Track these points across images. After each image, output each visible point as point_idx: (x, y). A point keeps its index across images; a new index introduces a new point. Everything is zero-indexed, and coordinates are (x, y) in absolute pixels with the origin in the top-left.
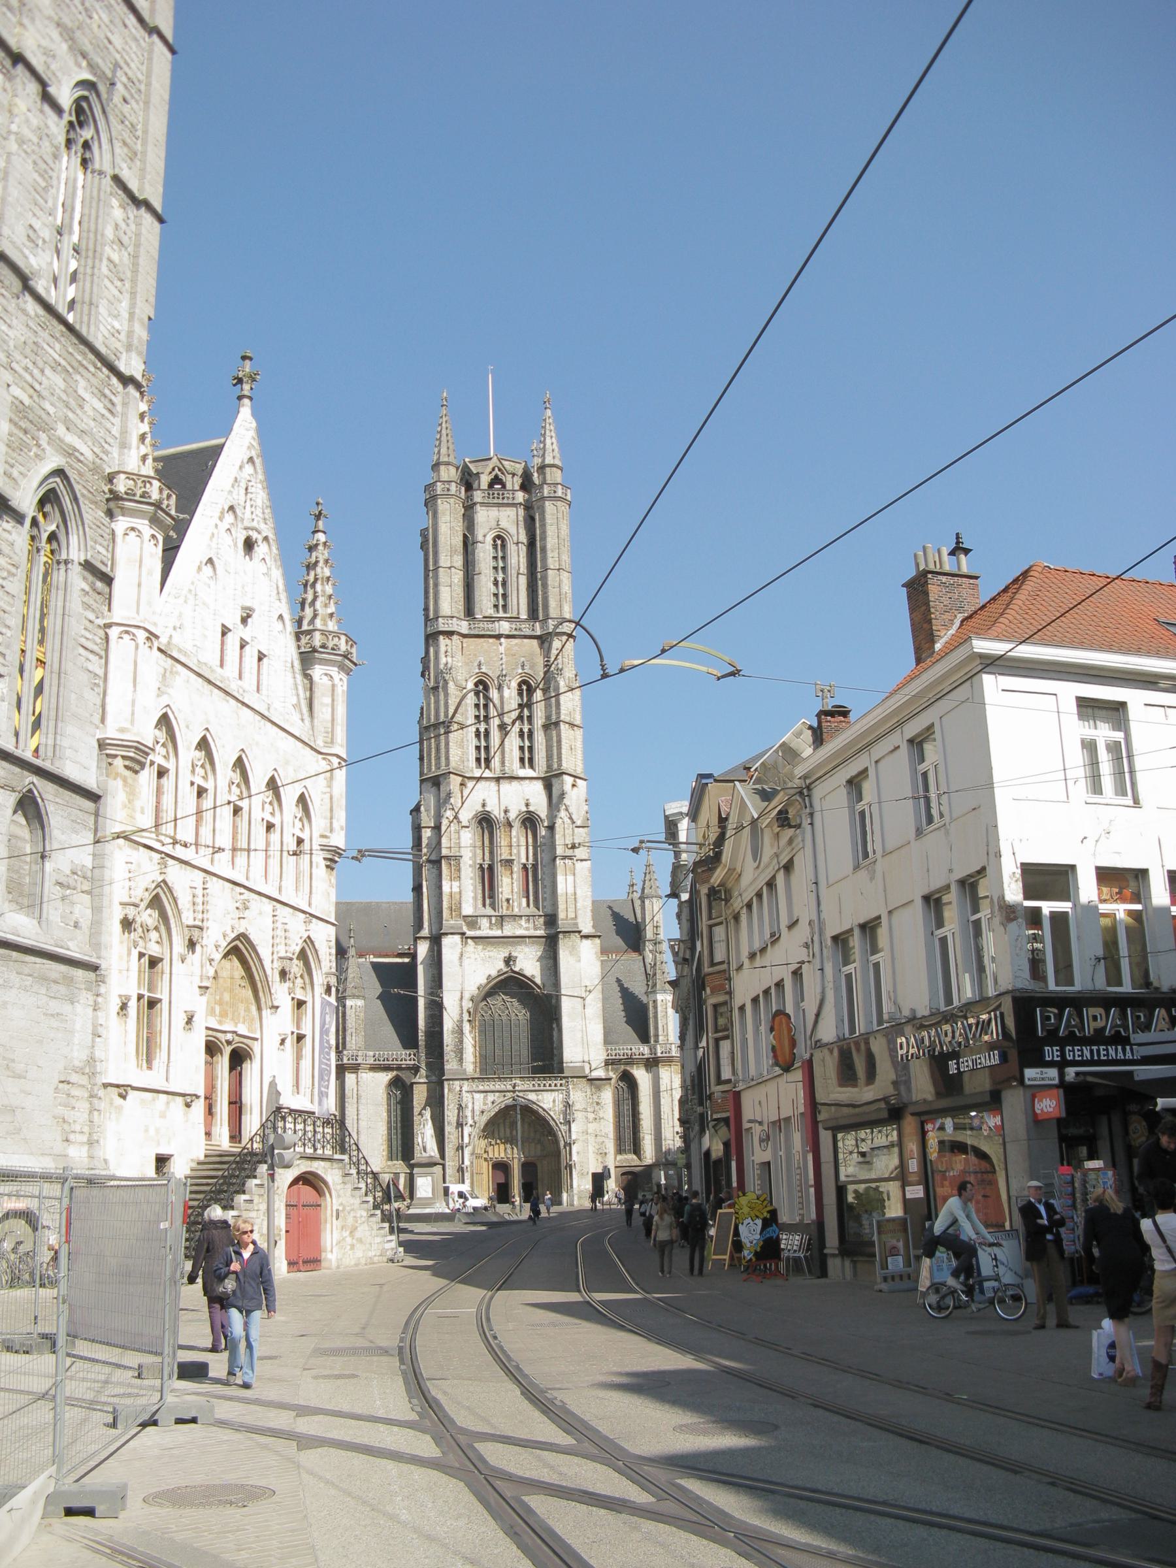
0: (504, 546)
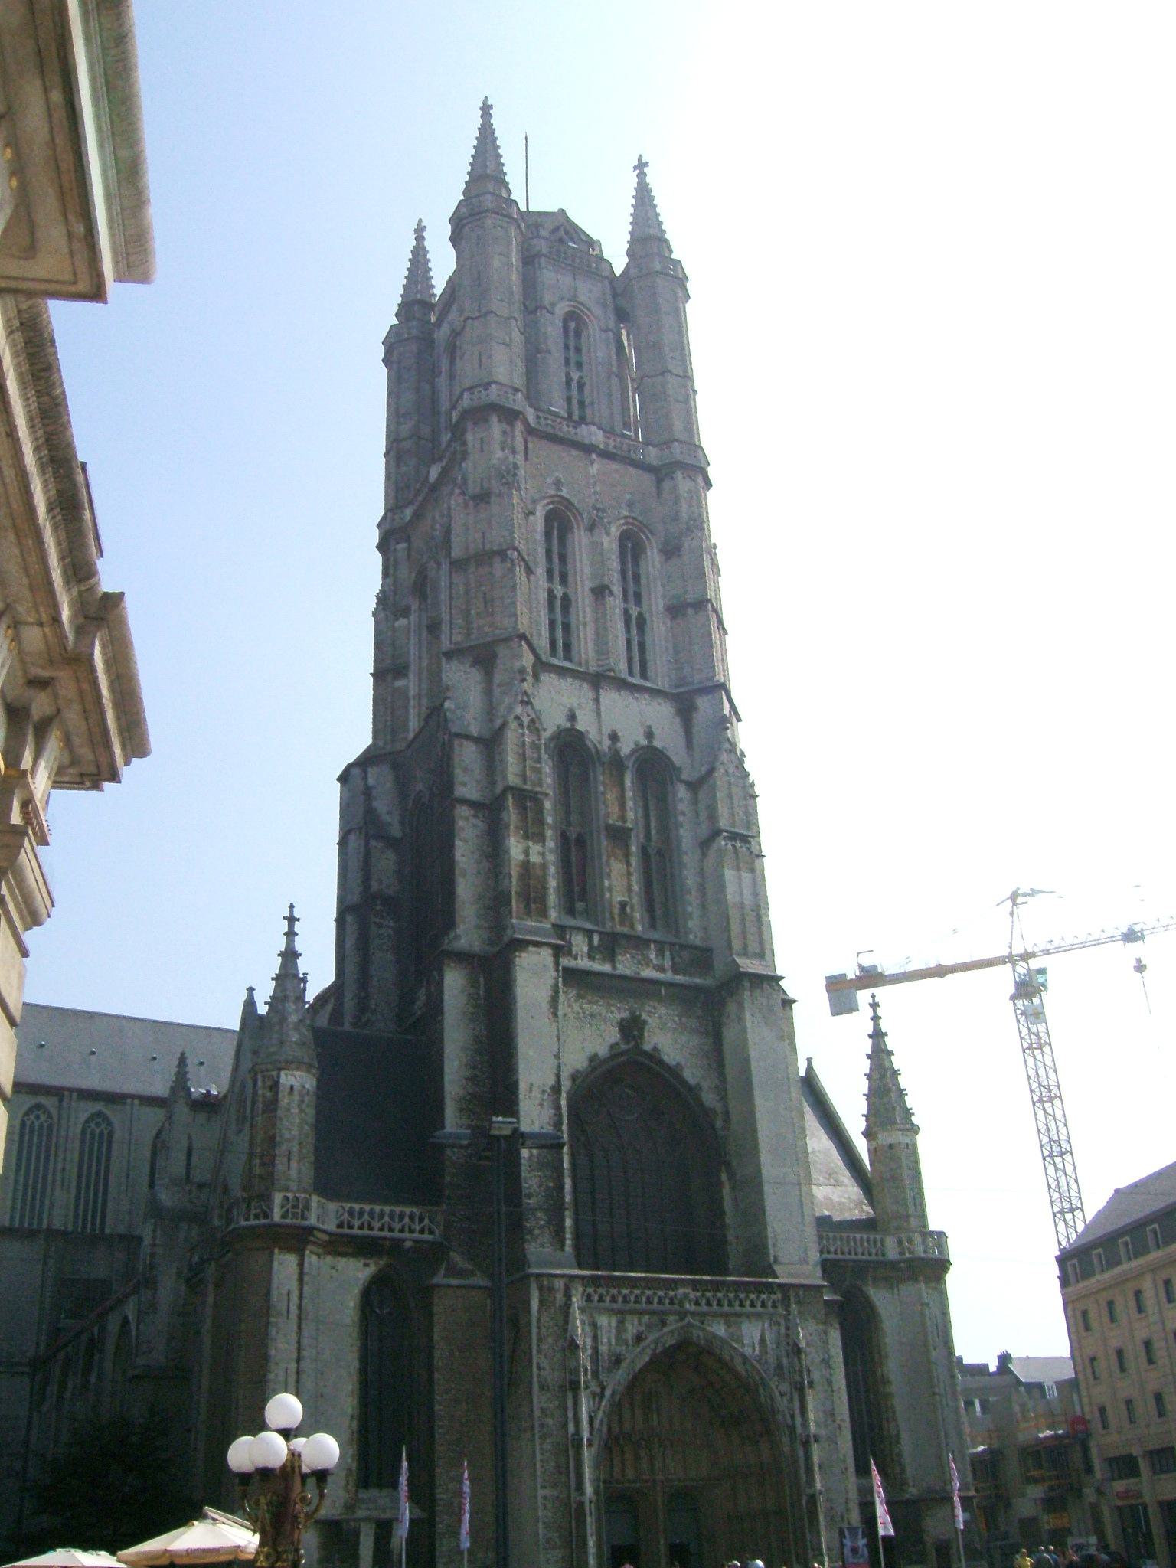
0: (578, 334)
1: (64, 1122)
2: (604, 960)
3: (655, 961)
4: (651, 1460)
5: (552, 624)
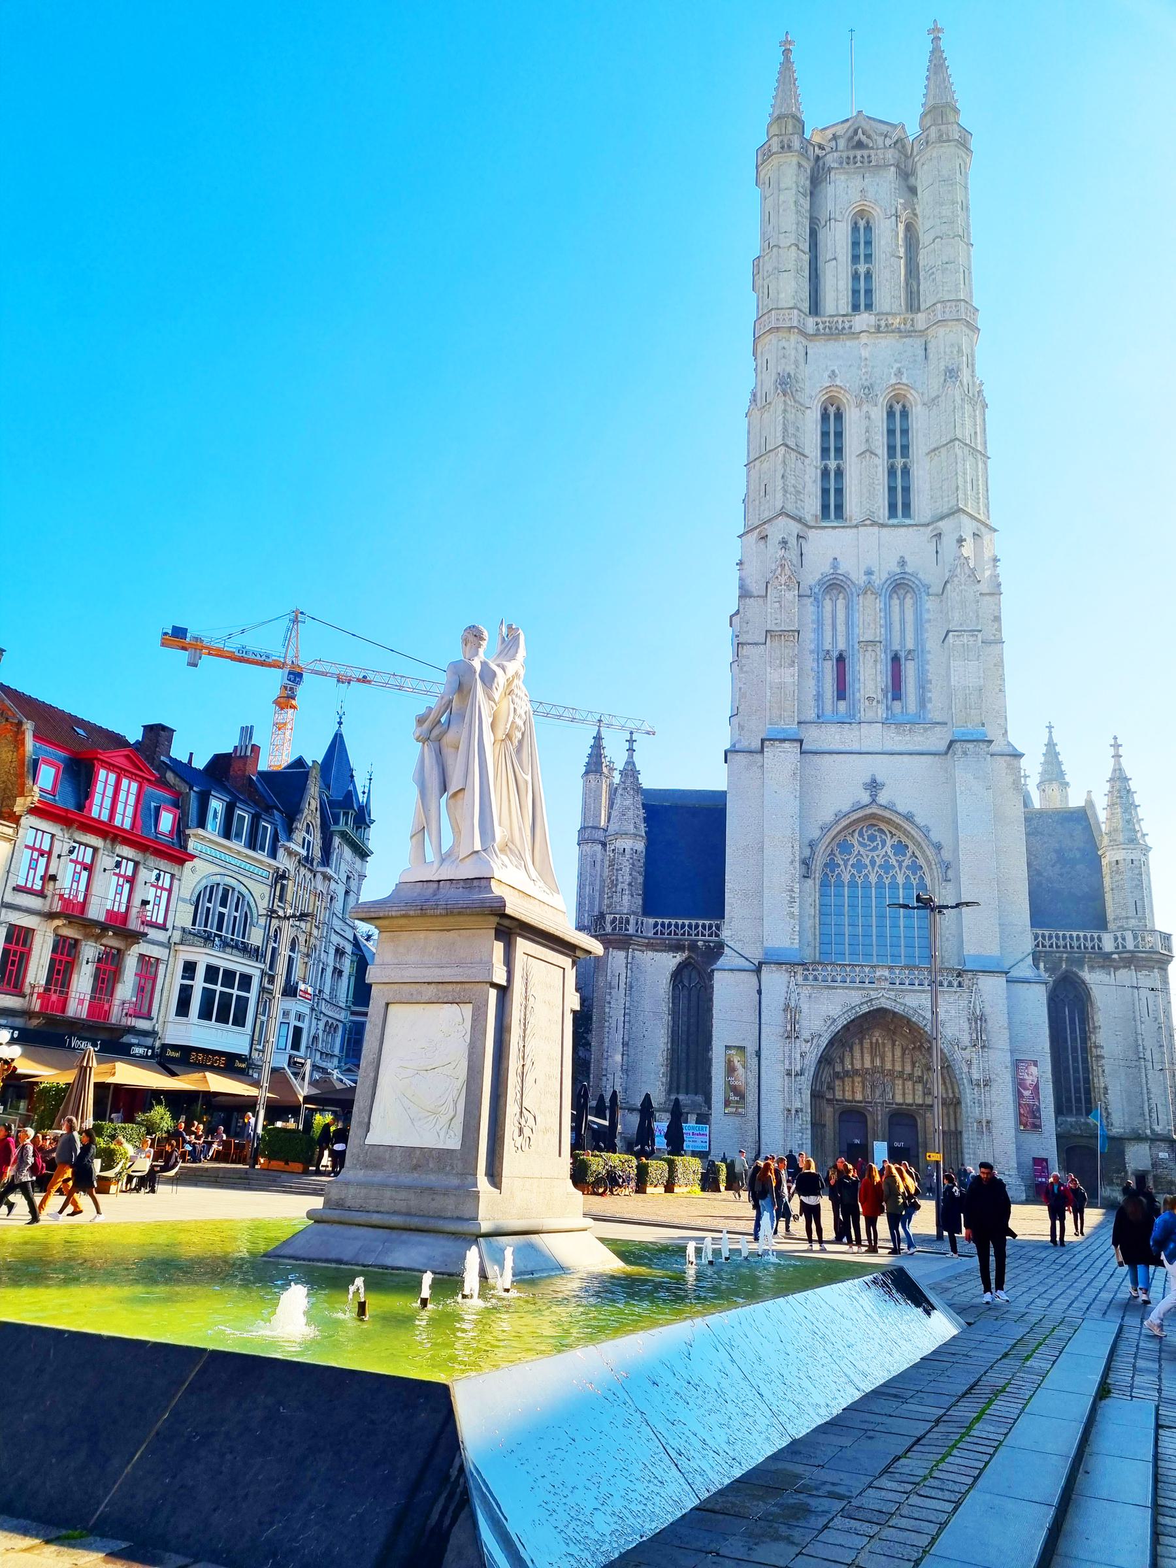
4: (873, 1087)
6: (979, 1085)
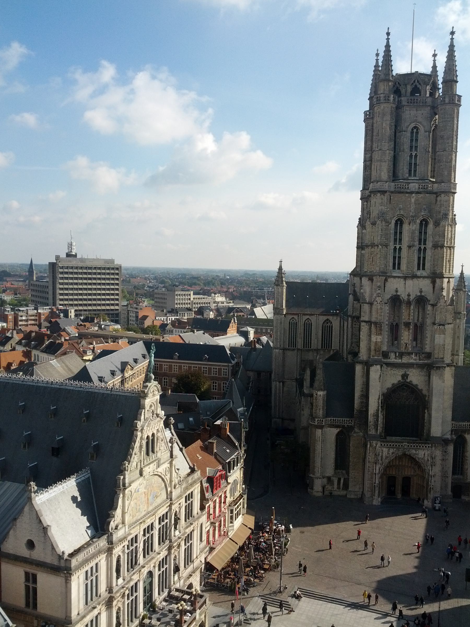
0: (417, 133)
1: (299, 322)
2: (399, 359)
3: (414, 358)
5: (394, 258)
6: (431, 477)
